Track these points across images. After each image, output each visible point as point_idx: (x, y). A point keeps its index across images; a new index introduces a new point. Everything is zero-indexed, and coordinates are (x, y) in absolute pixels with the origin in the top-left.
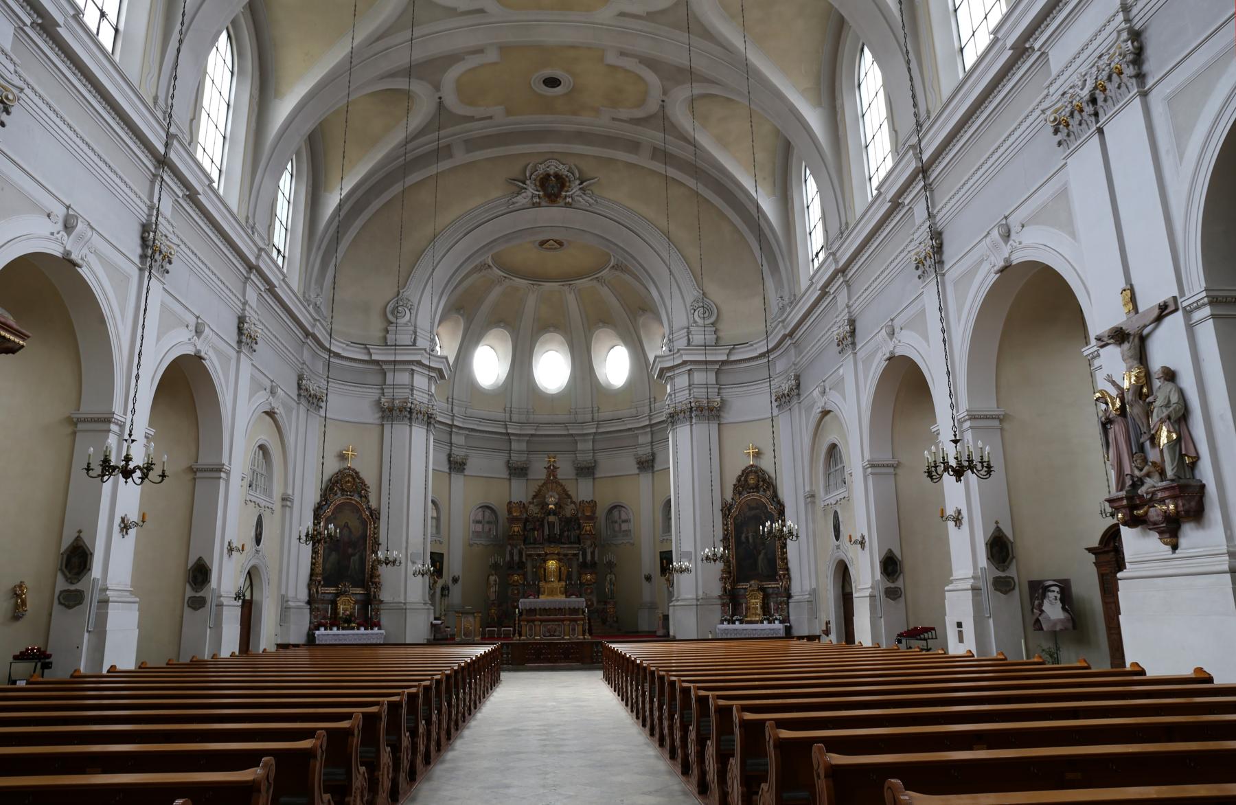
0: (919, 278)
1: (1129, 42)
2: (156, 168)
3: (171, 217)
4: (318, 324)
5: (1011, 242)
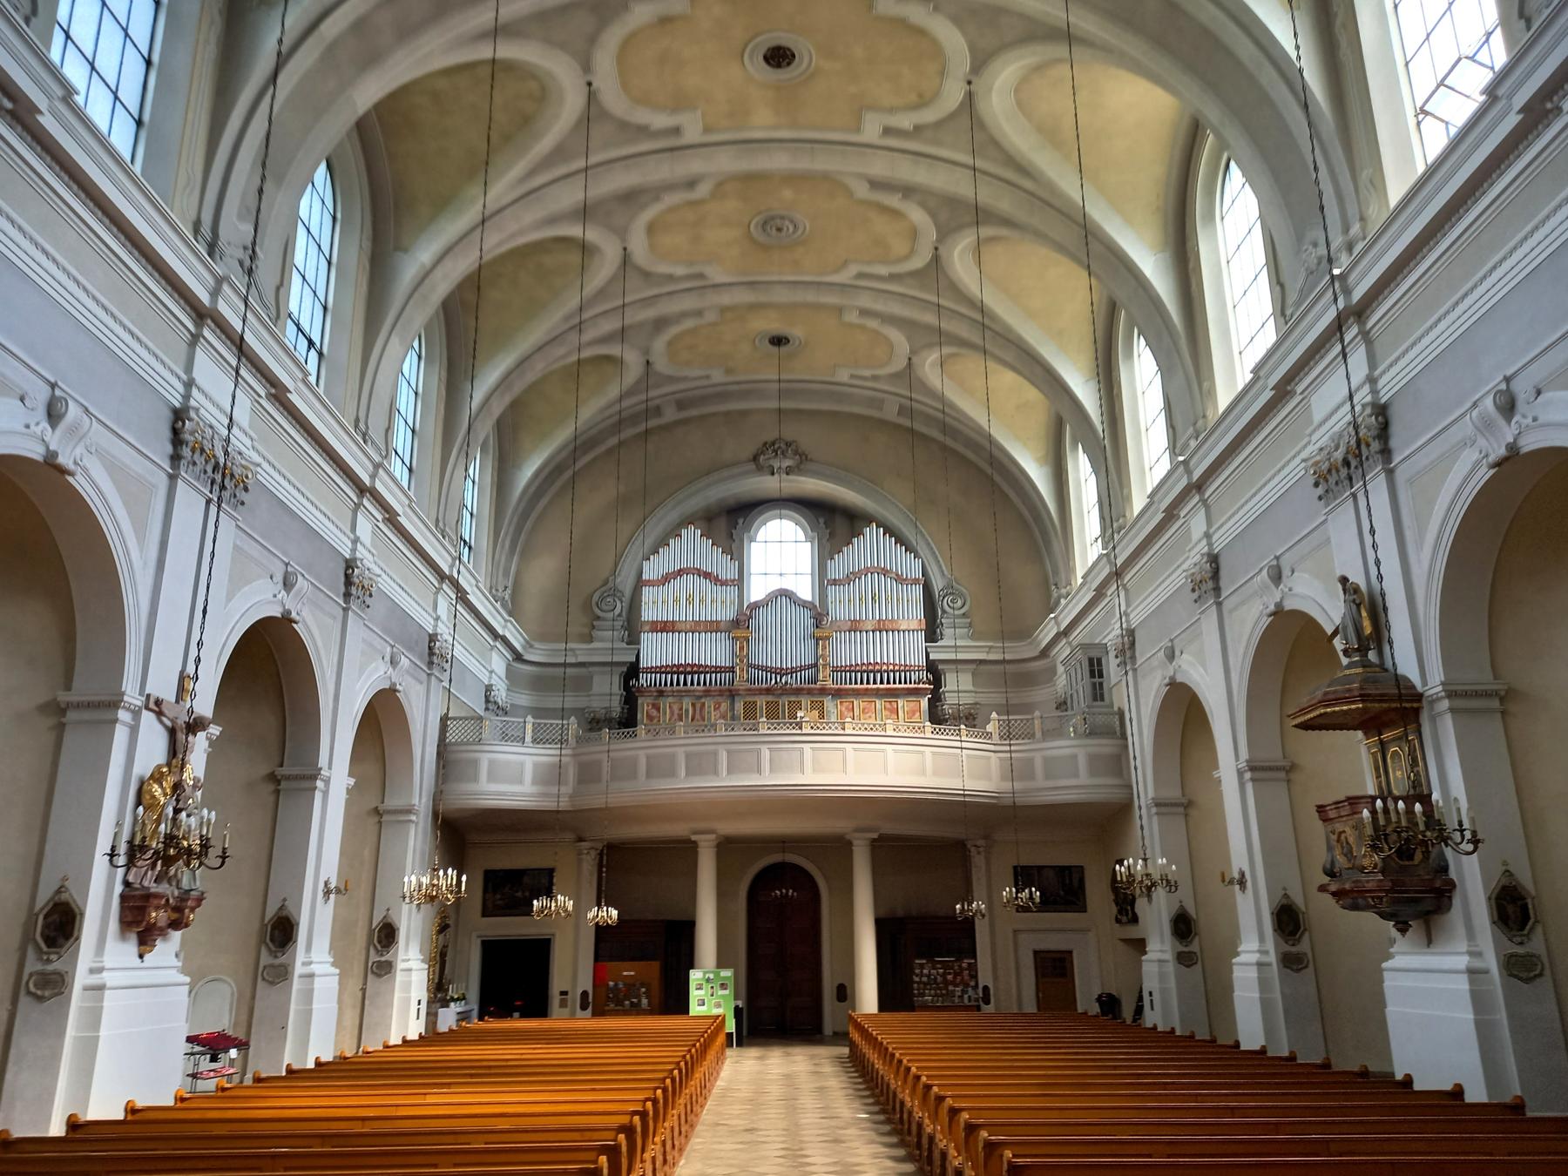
0: (1196, 601)
1: (1373, 417)
2: (358, 496)
3: (372, 546)
4: (509, 624)
5: (1281, 586)
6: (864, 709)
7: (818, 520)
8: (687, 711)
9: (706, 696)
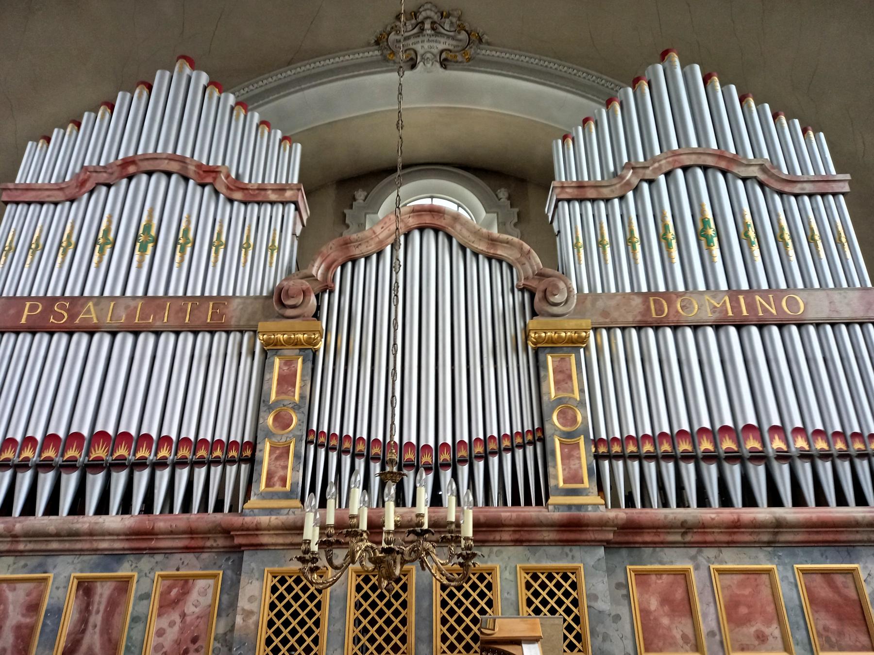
6: (732, 606)
7: (495, 191)
8: (56, 612)
9: (138, 552)
